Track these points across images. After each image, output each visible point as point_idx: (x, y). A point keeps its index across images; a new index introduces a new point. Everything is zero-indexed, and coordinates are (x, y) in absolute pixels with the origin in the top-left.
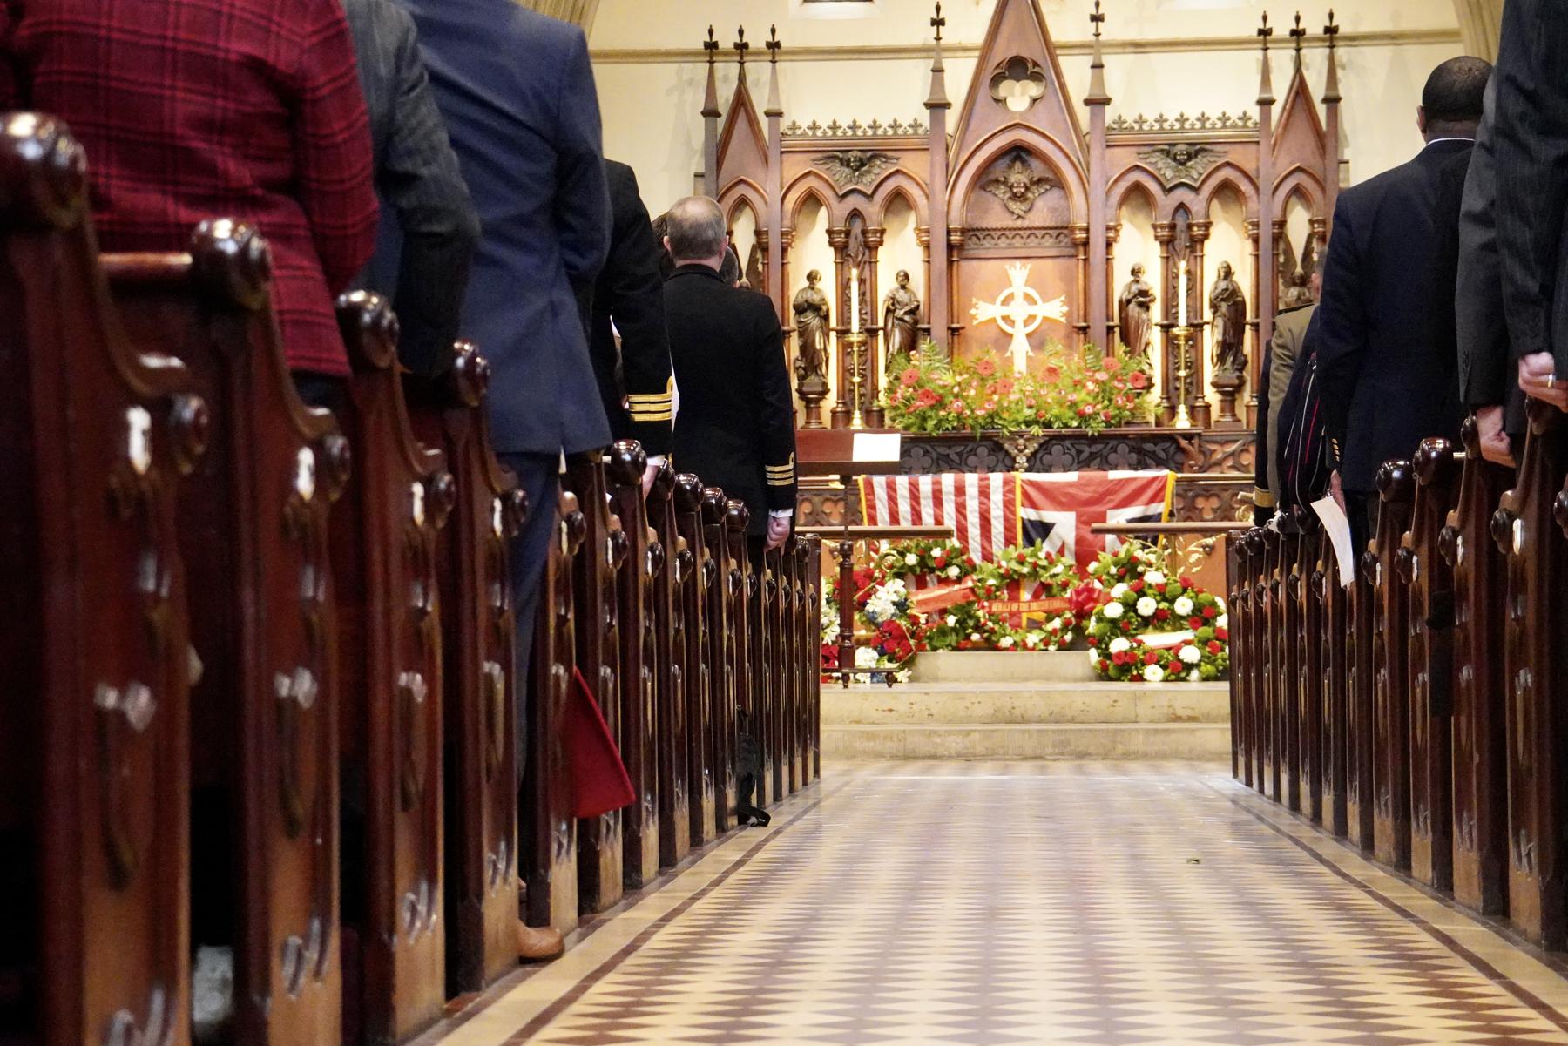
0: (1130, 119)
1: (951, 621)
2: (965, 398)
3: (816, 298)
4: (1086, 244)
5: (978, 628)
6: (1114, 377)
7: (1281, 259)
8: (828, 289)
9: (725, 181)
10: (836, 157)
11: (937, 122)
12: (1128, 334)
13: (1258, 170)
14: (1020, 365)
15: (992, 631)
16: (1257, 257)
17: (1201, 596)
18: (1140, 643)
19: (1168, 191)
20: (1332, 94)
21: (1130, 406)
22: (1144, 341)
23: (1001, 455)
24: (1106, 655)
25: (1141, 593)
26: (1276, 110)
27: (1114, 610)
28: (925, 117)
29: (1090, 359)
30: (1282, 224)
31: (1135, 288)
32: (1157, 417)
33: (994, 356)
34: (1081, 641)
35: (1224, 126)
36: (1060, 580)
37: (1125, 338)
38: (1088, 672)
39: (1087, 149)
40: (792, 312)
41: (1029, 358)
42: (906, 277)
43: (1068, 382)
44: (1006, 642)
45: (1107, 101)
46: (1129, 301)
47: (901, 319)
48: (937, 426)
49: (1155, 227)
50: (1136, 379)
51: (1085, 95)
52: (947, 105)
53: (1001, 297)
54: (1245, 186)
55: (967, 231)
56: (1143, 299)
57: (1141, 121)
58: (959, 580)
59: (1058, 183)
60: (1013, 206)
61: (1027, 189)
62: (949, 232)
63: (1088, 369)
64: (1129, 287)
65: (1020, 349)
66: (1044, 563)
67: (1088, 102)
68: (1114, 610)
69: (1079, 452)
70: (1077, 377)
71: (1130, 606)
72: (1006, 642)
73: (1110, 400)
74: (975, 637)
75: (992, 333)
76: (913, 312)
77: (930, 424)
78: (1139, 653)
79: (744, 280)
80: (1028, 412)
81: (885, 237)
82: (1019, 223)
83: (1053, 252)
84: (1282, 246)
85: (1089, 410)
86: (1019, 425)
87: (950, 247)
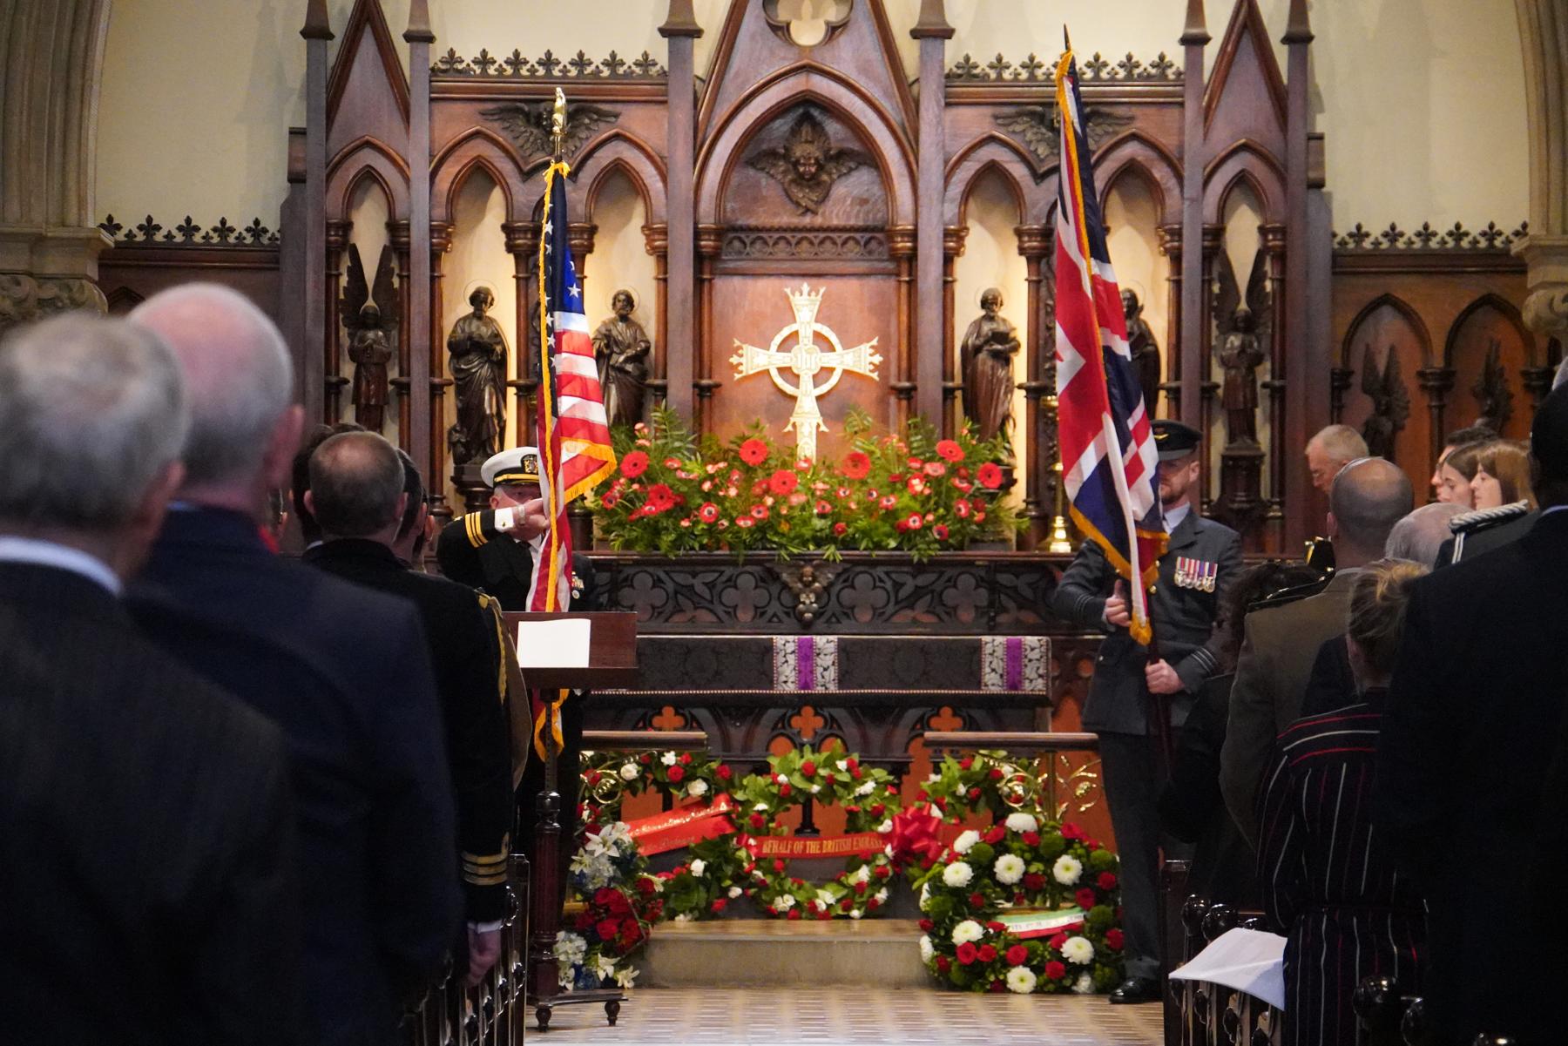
0: (983, 60)
1: (698, 867)
2: (721, 501)
3: (485, 331)
4: (912, 257)
5: (741, 878)
6: (954, 471)
7: (1216, 288)
8: (505, 315)
9: (338, 143)
10: (519, 110)
11: (680, 58)
12: (976, 397)
13: (1181, 146)
14: (807, 447)
15: (762, 885)
16: (1177, 284)
17: (1096, 853)
18: (1001, 929)
19: (1039, 177)
20: (1298, 29)
21: (978, 516)
22: (1000, 411)
23: (775, 589)
24: (944, 945)
25: (1001, 848)
26: (1211, 52)
27: (958, 874)
28: (660, 51)
29: (917, 440)
30: (1215, 234)
31: (987, 328)
32: (1019, 534)
33: (767, 432)
34: (899, 905)
35: (1129, 77)
36: (870, 804)
37: (971, 410)
38: (915, 971)
39: (912, 106)
40: (447, 354)
41: (820, 435)
42: (629, 301)
43: (883, 478)
44: (785, 902)
45: (948, 33)
46: (978, 350)
47: (621, 370)
48: (676, 545)
49: (1019, 233)
50: (988, 474)
51: (913, 23)
52: (698, 33)
53: (778, 339)
54: (1160, 172)
55: (726, 231)
56: (999, 345)
57: (999, 64)
58: (705, 801)
59: (870, 157)
60: (798, 194)
61: (821, 167)
62: (698, 234)
63: (913, 458)
64: (978, 324)
65: (807, 423)
66: (845, 778)
67: (916, 34)
68: (958, 874)
69: (898, 586)
70: (898, 471)
71: (982, 866)
72: (785, 902)
73: (948, 509)
74: (736, 892)
75: (763, 392)
76: (639, 358)
77: (667, 539)
78: (998, 945)
79: (370, 302)
80: (818, 523)
81: (597, 239)
82: (807, 220)
83: (862, 266)
84: (1216, 269)
85: (914, 522)
86: (805, 543)
87: (699, 258)
